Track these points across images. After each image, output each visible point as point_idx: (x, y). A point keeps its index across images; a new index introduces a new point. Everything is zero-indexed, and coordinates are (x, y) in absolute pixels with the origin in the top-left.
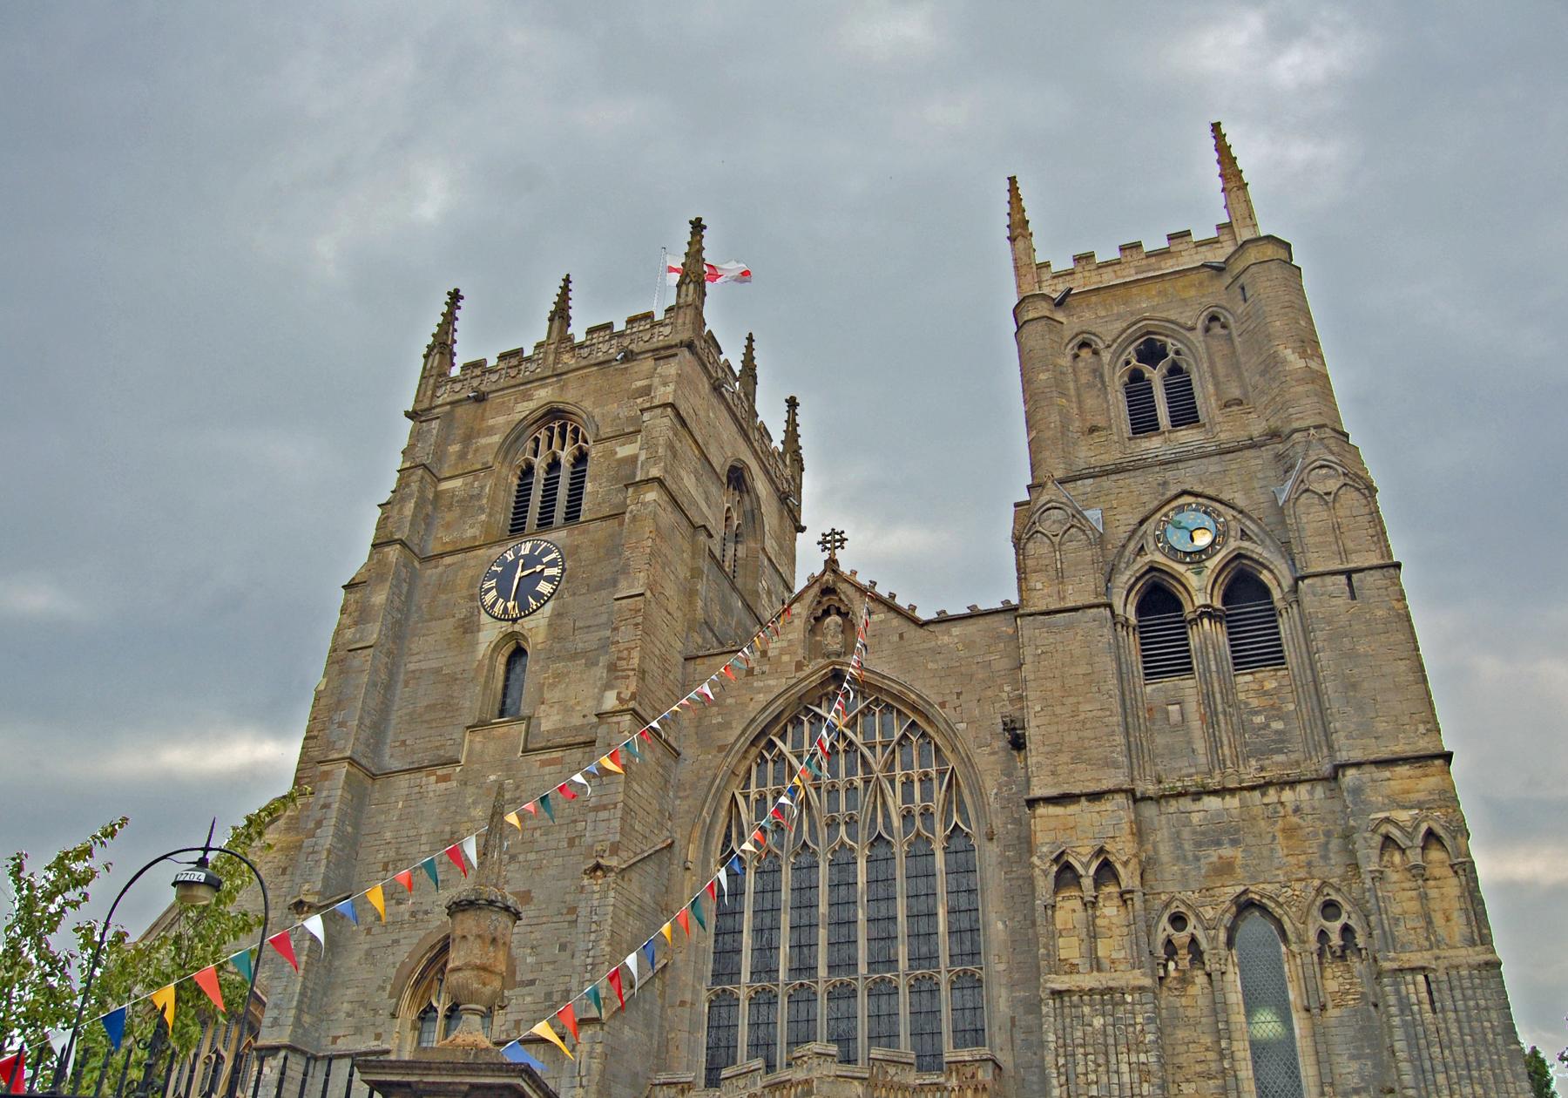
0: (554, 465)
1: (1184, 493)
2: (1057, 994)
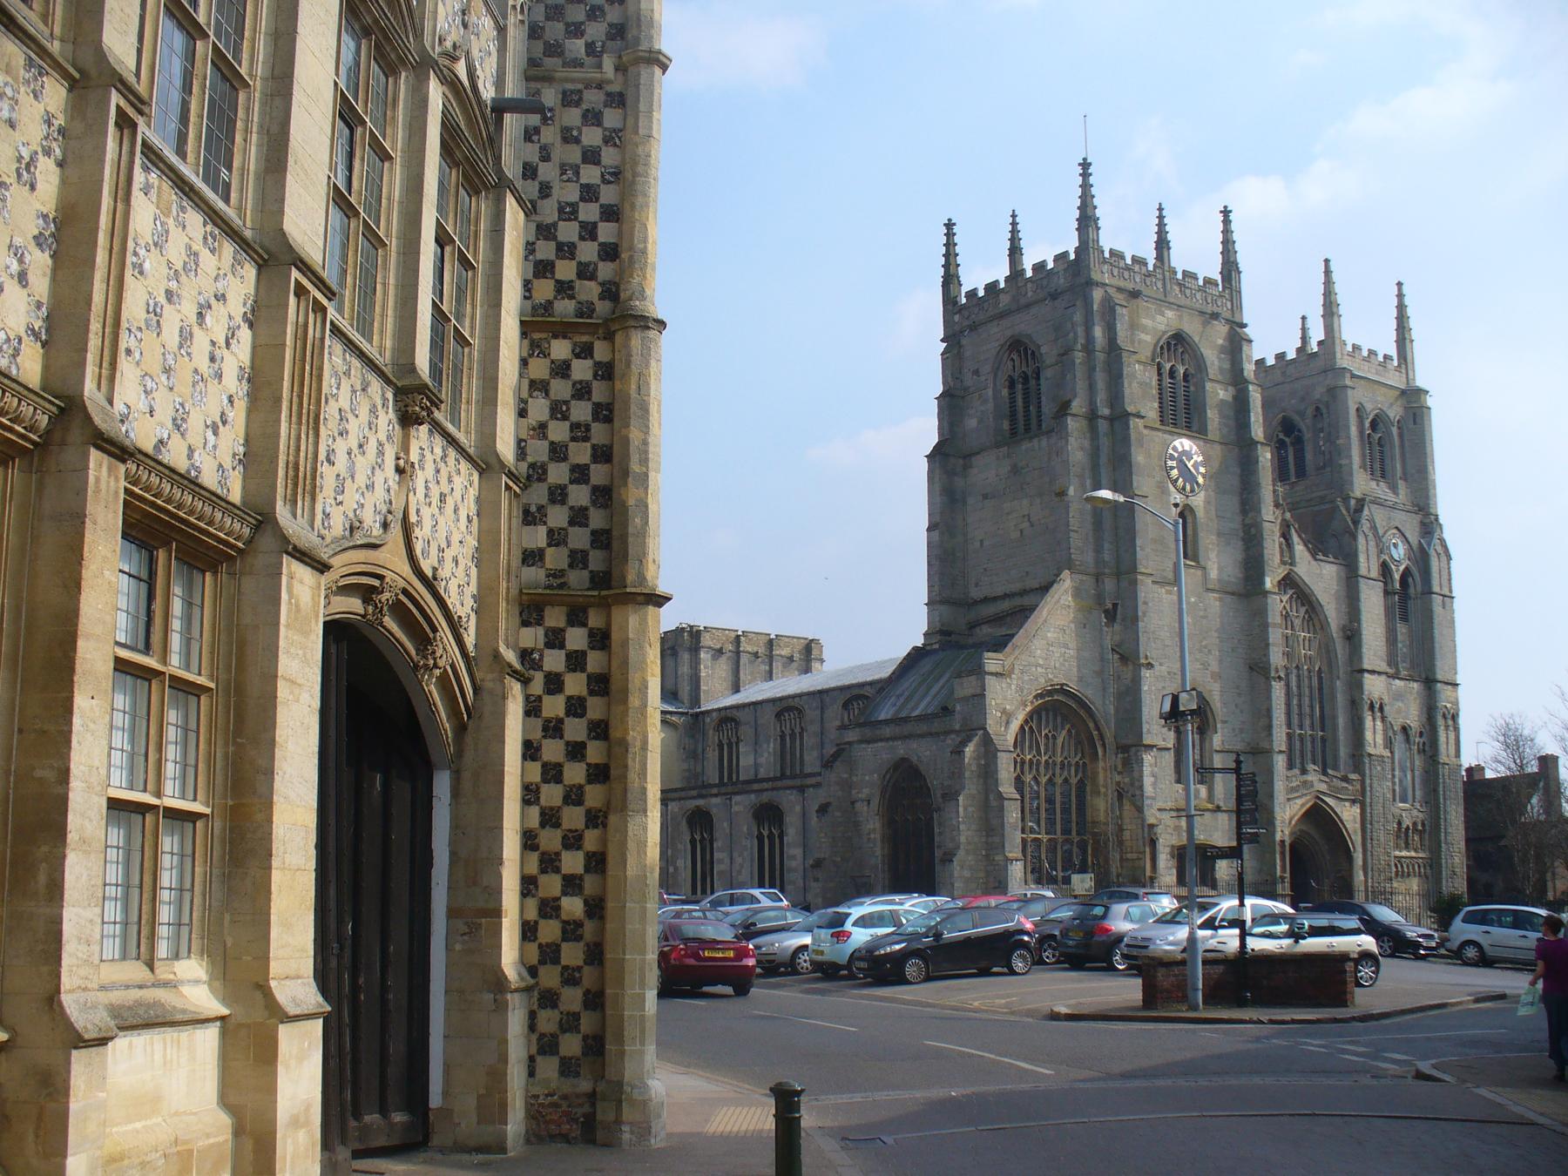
0: (1172, 373)
1: (1397, 528)
2: (1370, 755)
